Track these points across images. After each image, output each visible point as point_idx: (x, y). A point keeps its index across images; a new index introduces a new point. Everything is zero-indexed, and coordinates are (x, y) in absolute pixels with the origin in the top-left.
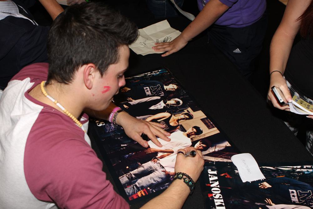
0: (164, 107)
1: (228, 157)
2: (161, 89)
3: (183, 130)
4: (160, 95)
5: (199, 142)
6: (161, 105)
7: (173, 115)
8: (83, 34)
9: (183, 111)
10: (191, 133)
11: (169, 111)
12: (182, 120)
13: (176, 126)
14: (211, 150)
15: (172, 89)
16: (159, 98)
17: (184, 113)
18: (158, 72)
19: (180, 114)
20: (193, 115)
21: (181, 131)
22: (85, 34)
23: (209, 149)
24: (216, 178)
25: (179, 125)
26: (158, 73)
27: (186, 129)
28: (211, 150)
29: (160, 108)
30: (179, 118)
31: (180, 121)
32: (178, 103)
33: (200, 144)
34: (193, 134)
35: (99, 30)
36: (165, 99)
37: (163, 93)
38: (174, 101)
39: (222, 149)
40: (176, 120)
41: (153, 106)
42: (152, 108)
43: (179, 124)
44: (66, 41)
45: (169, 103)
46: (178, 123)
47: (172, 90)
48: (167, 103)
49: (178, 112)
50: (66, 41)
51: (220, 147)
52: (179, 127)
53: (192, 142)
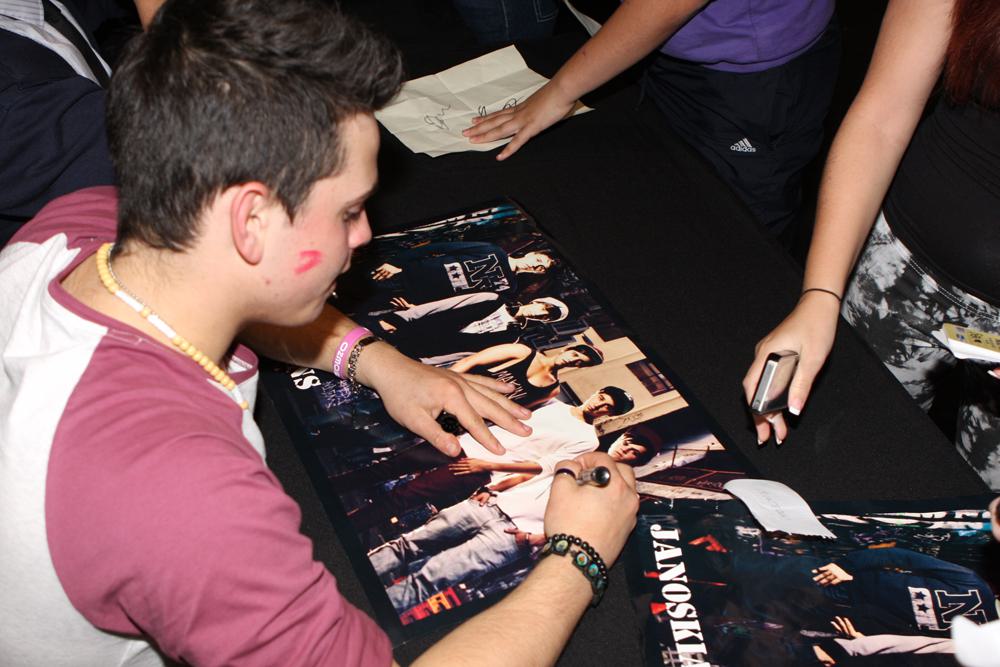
0: (511, 325)
1: (715, 485)
2: (498, 269)
3: (572, 399)
4: (498, 286)
5: (623, 437)
6: (501, 320)
7: (538, 353)
8: (222, 86)
9: (569, 338)
10: (597, 408)
11: (525, 338)
12: (567, 369)
13: (548, 387)
14: (662, 462)
15: (535, 268)
16: (493, 296)
17: (574, 345)
18: (490, 213)
19: (562, 349)
20: (601, 353)
21: (566, 403)
22: (227, 87)
23: (654, 459)
24: (677, 552)
26: (491, 217)
27: (580, 396)
28: (662, 462)
30: (559, 362)
31: (559, 372)
32: (554, 312)
33: (626, 444)
34: (603, 413)
35: (273, 71)
36: (511, 300)
37: (505, 280)
38: (543, 306)
39: (695, 458)
40: (547, 369)
41: (476, 323)
42: (473, 328)
44: (166, 110)
45: (525, 314)
46: (556, 378)
47: (535, 272)
48: (519, 314)
49: (554, 342)
50: (166, 110)
51: (689, 452)
52: (558, 389)
53: (600, 438)
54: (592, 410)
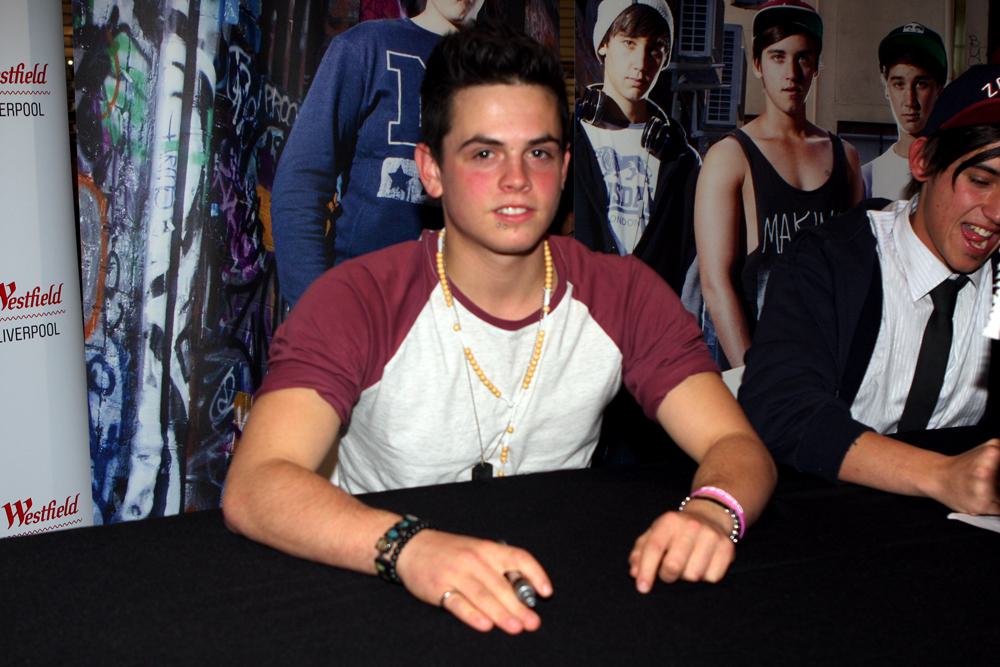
0: (648, 142)
10: (915, 105)
12: (810, 98)
17: (748, 39)
25: (836, 141)
27: (879, 118)
29: (653, 184)
30: (786, 101)
31: (811, 116)
38: (618, 43)
40: (795, 138)
41: (612, 215)
43: (830, 135)
45: (632, 92)
46: (820, 133)
48: (625, 108)
49: (727, 79)
52: (848, 146)
54: (915, 118)
